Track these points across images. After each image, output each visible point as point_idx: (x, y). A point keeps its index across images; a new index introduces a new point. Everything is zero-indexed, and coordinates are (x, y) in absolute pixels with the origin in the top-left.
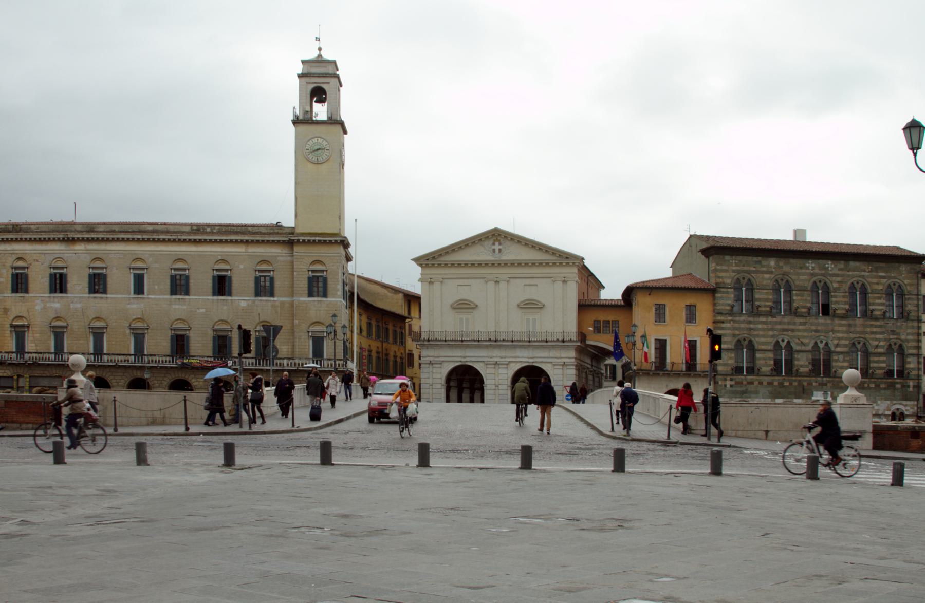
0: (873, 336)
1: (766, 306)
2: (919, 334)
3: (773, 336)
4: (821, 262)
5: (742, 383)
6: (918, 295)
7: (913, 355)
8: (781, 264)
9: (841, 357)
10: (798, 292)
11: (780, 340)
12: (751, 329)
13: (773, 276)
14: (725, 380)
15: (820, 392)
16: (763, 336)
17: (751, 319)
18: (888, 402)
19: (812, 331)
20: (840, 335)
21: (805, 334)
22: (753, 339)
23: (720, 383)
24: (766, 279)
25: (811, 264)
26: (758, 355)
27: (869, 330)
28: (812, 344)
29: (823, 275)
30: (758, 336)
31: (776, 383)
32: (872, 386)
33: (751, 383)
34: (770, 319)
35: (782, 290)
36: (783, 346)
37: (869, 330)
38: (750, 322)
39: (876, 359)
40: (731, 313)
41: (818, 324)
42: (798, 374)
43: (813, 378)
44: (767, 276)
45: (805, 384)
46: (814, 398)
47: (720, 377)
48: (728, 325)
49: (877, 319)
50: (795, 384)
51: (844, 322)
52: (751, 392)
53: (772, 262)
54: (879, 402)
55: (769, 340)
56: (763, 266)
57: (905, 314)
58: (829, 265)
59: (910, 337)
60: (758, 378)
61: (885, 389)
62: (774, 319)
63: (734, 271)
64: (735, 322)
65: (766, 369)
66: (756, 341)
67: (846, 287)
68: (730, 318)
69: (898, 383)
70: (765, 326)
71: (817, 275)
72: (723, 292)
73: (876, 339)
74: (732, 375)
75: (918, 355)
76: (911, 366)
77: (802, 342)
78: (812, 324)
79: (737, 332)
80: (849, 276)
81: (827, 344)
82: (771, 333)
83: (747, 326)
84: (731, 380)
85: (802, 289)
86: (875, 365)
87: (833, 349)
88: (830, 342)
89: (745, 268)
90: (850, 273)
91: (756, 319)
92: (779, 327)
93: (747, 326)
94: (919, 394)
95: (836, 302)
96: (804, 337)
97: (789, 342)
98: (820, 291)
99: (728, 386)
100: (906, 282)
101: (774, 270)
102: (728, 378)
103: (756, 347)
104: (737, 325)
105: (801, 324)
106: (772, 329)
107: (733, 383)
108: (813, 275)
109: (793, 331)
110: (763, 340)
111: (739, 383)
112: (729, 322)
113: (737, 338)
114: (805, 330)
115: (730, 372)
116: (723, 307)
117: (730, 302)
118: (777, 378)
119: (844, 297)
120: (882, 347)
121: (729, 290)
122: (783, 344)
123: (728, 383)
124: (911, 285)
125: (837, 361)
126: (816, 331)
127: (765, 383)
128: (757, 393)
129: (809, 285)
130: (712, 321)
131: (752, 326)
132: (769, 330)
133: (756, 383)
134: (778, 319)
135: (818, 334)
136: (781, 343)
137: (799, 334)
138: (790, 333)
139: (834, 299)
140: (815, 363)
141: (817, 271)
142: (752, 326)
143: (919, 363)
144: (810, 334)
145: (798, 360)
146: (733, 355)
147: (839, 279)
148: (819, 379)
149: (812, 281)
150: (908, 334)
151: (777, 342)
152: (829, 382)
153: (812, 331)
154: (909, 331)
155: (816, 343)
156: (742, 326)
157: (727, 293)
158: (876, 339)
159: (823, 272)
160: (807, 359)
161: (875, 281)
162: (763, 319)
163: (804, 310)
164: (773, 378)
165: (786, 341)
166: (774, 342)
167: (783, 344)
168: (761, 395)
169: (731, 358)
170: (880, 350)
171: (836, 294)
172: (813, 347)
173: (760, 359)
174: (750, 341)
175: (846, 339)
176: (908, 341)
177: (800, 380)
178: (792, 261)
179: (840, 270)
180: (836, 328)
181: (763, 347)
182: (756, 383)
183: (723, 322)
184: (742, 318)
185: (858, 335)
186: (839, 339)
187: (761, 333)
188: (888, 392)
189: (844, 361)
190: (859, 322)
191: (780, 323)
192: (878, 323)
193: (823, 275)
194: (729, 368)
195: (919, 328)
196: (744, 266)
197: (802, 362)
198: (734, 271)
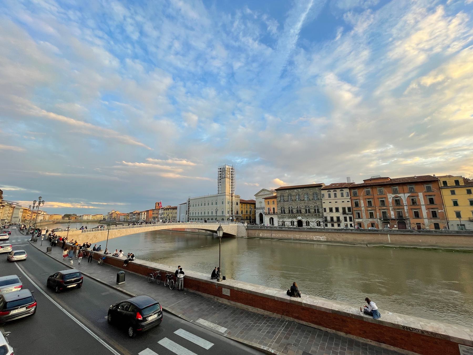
0: (310, 204)
3: (288, 206)
4: (297, 189)
8: (289, 191)
9: (303, 209)
16: (286, 206)
19: (296, 204)
20: (302, 204)
25: (295, 190)
27: (309, 203)
30: (285, 206)
34: (287, 202)
38: (283, 203)
40: (280, 202)
52: (284, 217)
58: (299, 190)
61: (314, 216)
64: (280, 204)
71: (297, 192)
73: (311, 205)
78: (296, 203)
81: (300, 206)
82: (288, 205)
83: (283, 204)
86: (311, 210)
93: (283, 204)
105: (294, 203)
106: (288, 204)
109: (292, 204)
111: (282, 216)
112: (279, 204)
114: (295, 204)
122: (291, 207)
123: (280, 216)
132: (287, 205)
133: (285, 216)
134: (289, 202)
151: (289, 207)
153: (296, 204)
154: (319, 202)
158: (311, 205)
162: (286, 203)
167: (291, 207)
168: (286, 218)
173: (286, 211)
175: (304, 205)
176: (319, 205)
182: (285, 216)
186: (302, 205)
188: (315, 217)
191: (289, 203)
197: (295, 211)
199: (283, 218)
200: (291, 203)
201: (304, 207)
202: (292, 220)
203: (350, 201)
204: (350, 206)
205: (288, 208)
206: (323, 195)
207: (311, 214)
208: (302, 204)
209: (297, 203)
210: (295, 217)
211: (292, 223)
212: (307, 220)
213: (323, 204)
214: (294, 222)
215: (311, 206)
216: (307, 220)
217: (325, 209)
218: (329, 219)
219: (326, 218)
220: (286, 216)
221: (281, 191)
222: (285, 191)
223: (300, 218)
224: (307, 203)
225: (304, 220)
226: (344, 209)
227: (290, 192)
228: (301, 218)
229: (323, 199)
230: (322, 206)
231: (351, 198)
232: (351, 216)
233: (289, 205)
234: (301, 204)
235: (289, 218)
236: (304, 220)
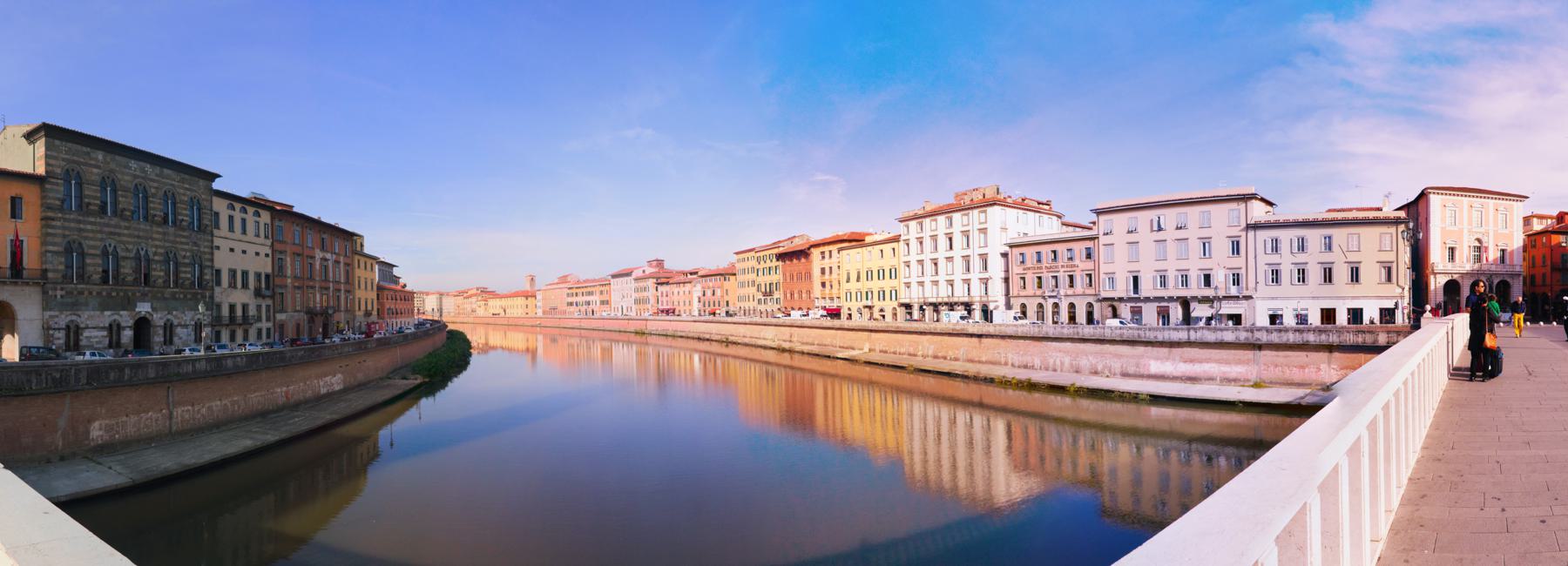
1: (95, 204)
2: (212, 248)
3: (101, 240)
5: (72, 293)
6: (211, 210)
7: (209, 266)
10: (124, 193)
11: (107, 245)
12: (80, 230)
13: (100, 171)
14: (56, 289)
15: (146, 304)
16: (92, 239)
17: (81, 218)
18: (193, 312)
20: (157, 243)
21: (129, 240)
22: (83, 242)
23: (50, 293)
24: (94, 174)
25: (133, 164)
26: (88, 261)
27: (178, 239)
28: (134, 252)
29: (143, 178)
30: (86, 238)
31: (104, 293)
32: (182, 296)
33: (81, 293)
34: (98, 220)
35: (109, 189)
36: (110, 251)
37: (178, 239)
38: (79, 222)
39: (184, 269)
40: (61, 209)
41: (139, 230)
42: (124, 283)
43: (137, 288)
44: (95, 170)
45: (130, 294)
46: (137, 310)
47: (51, 286)
48: (58, 223)
49: (183, 229)
50: (122, 294)
51: (160, 230)
53: (100, 156)
54: (186, 313)
55: (99, 243)
56: (91, 159)
57: (203, 228)
58: (148, 167)
59: (206, 250)
60: (88, 287)
61: (190, 299)
62: (102, 221)
63: (63, 160)
64: (65, 220)
65: (96, 277)
66: (86, 243)
67: (161, 193)
68: (60, 215)
69: (198, 293)
70: (94, 228)
71: (138, 177)
72: (53, 184)
74: (62, 283)
75: (212, 267)
76: (207, 277)
78: (135, 229)
79: (67, 233)
80: (164, 183)
82: (99, 236)
84: (62, 289)
85: (126, 190)
87: (151, 256)
88: (149, 249)
89: (75, 158)
90: (164, 180)
91: (86, 219)
92: (106, 229)
94: (212, 305)
95: (154, 209)
96: (128, 243)
97: (115, 247)
98: (141, 195)
99: (59, 297)
100: (203, 196)
102: (59, 287)
103: (86, 250)
104: (66, 224)
106: (100, 232)
107: (63, 293)
108: (135, 177)
110: (92, 243)
111: (70, 293)
112: (59, 219)
113: (67, 240)
114: (130, 236)
115: (60, 281)
116: (52, 201)
117: (59, 196)
118: (105, 287)
119: (160, 204)
120: (188, 258)
121: (59, 181)
123: (59, 293)
124: (207, 201)
125: (155, 270)
126: (138, 237)
127: (94, 293)
128: (87, 304)
129: (131, 186)
130: (39, 218)
131: (82, 226)
133: (86, 293)
134: (106, 220)
135: (140, 241)
136: (108, 248)
137: (125, 239)
138: (118, 239)
139: (152, 205)
140: (137, 270)
141: (138, 173)
142: (82, 226)
143: (212, 274)
144: (133, 240)
145: (124, 267)
146: (63, 260)
147: (155, 185)
148: (141, 288)
149: (134, 184)
150: (205, 247)
152: (149, 291)
154: (206, 244)
155: (138, 250)
156: (72, 225)
157: (57, 184)
159: (143, 175)
160: (132, 268)
161: (182, 191)
163: (128, 213)
164: (101, 287)
165: (113, 245)
166: (101, 247)
169: (61, 263)
170: (187, 261)
171: (154, 200)
172: (136, 254)
173: (89, 265)
174: (80, 244)
176: (205, 253)
177: (125, 290)
178: (118, 158)
179: (157, 175)
180: (155, 236)
181: (92, 251)
182: (86, 293)
183: (53, 219)
184: (72, 216)
185: (170, 245)
186: (156, 247)
187: (91, 235)
189: (161, 270)
190: (171, 230)
191: (108, 225)
192: (185, 234)
193: (143, 178)
194: (60, 275)
195: (212, 241)
196: (73, 155)
198: (63, 160)
199: (74, 306)
200: (116, 226)
201: (161, 254)
202: (116, 317)
203: (270, 255)
204: (269, 270)
205: (98, 252)
206: (217, 214)
207: (181, 293)
208: (157, 243)
209: (136, 233)
210: (129, 304)
211: (114, 329)
212: (169, 317)
213: (216, 252)
214: (124, 328)
215: (184, 257)
216: (169, 317)
217: (218, 272)
218: (225, 312)
219: (219, 306)
220: (91, 293)
221: (69, 145)
222: (88, 153)
223: (144, 308)
224: (172, 238)
225: (159, 316)
226: (258, 275)
227: (113, 166)
228: (150, 310)
229: (216, 232)
230: (212, 260)
231: (272, 243)
232: (270, 302)
233: (104, 236)
234: (153, 239)
235: (103, 307)
236: (158, 319)
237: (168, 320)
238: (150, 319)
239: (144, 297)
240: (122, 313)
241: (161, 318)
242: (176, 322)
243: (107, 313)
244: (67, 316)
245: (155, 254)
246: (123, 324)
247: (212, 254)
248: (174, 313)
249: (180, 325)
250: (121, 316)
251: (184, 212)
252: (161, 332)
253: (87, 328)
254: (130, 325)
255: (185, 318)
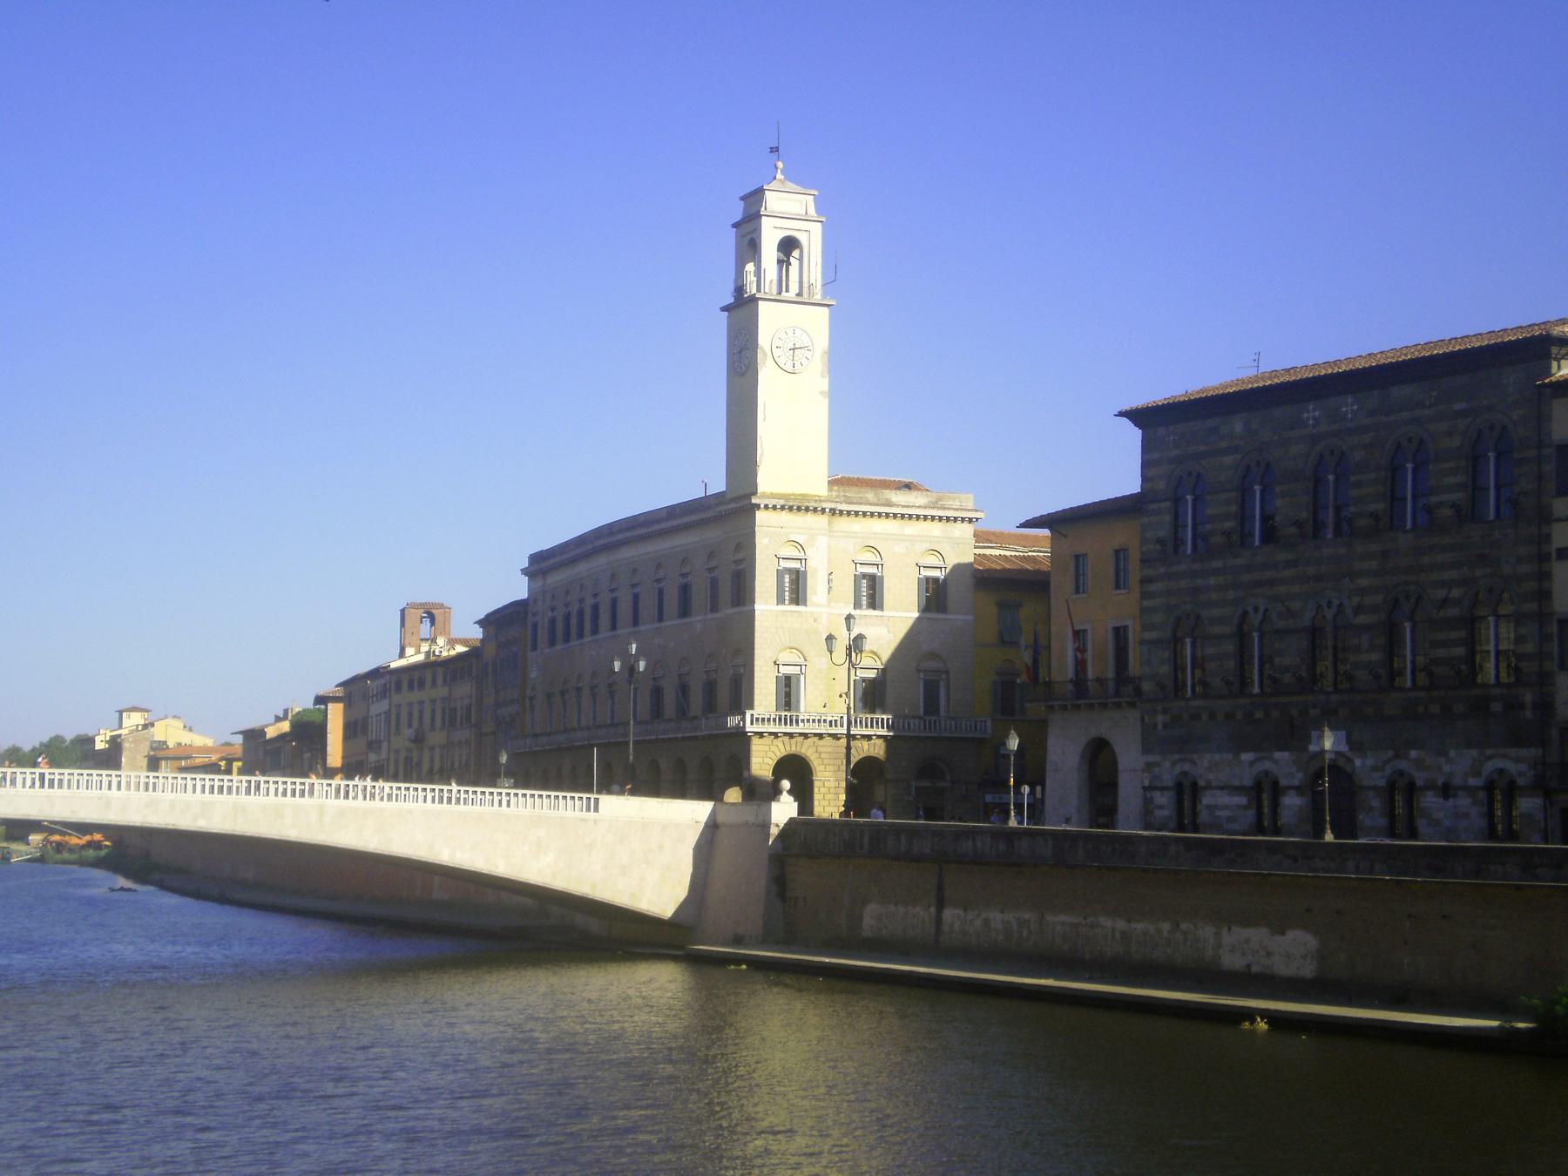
2: (1543, 558)
11: (1250, 609)
17: (1197, 567)
18: (1474, 753)
20: (1364, 582)
21: (1296, 589)
27: (1426, 560)
31: (1239, 715)
37: (1426, 560)
53: (1237, 425)
54: (1452, 754)
58: (1348, 406)
62: (1239, 561)
68: (1162, 570)
77: (1288, 609)
82: (1231, 594)
84: (1165, 711)
92: (1246, 577)
99: (1160, 727)
101: (1242, 443)
110: (1216, 612)
123: (1160, 719)
131: (1199, 582)
133: (1205, 716)
137: (1283, 589)
142: (1199, 582)
162: (1217, 564)
165: (1262, 609)
182: (1205, 716)
195: (1548, 538)
202: (1267, 765)
211: (1265, 791)
215: (1445, 602)
216: (1403, 765)
225: (1370, 762)
230: (1544, 595)
236: (1369, 769)
237: (1401, 773)
238: (1349, 769)
239: (1329, 717)
240: (1277, 755)
241: (1375, 769)
242: (1420, 778)
243: (1246, 757)
244: (1174, 764)
245: (1359, 610)
246: (1283, 782)
247: (1545, 576)
248: (1413, 754)
249: (1430, 786)
250: (1276, 762)
251: (1451, 480)
252: (1376, 803)
253: (1208, 787)
254: (1296, 783)
255: (1447, 768)
